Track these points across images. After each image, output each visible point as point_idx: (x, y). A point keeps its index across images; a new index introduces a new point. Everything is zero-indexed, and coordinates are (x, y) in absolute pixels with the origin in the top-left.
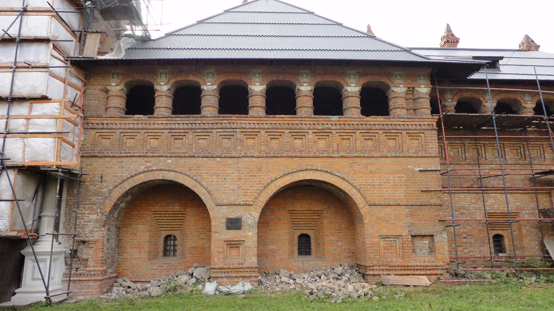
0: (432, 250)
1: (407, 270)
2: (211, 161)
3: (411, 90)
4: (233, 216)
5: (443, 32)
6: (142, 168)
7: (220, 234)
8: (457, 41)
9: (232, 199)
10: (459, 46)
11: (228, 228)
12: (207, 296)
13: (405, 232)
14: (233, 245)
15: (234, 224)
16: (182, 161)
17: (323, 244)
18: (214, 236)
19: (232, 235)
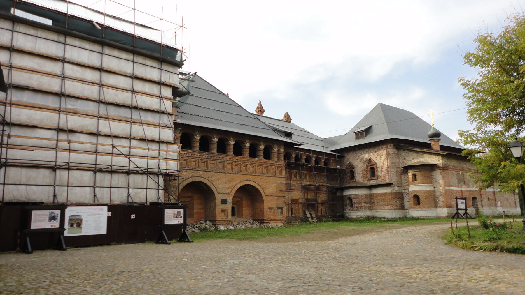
0: (282, 213)
1: (276, 221)
2: (216, 174)
3: (279, 150)
4: (224, 198)
5: (257, 105)
6: (191, 175)
7: (220, 206)
8: (263, 111)
9: (223, 191)
10: (264, 114)
11: (222, 203)
12: (220, 231)
13: (275, 206)
14: (223, 211)
15: (224, 202)
16: (205, 173)
17: (242, 211)
18: (218, 207)
19: (223, 206)
